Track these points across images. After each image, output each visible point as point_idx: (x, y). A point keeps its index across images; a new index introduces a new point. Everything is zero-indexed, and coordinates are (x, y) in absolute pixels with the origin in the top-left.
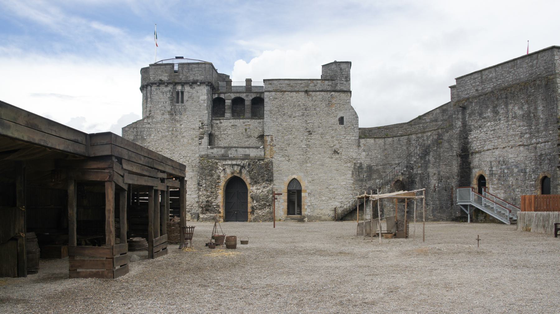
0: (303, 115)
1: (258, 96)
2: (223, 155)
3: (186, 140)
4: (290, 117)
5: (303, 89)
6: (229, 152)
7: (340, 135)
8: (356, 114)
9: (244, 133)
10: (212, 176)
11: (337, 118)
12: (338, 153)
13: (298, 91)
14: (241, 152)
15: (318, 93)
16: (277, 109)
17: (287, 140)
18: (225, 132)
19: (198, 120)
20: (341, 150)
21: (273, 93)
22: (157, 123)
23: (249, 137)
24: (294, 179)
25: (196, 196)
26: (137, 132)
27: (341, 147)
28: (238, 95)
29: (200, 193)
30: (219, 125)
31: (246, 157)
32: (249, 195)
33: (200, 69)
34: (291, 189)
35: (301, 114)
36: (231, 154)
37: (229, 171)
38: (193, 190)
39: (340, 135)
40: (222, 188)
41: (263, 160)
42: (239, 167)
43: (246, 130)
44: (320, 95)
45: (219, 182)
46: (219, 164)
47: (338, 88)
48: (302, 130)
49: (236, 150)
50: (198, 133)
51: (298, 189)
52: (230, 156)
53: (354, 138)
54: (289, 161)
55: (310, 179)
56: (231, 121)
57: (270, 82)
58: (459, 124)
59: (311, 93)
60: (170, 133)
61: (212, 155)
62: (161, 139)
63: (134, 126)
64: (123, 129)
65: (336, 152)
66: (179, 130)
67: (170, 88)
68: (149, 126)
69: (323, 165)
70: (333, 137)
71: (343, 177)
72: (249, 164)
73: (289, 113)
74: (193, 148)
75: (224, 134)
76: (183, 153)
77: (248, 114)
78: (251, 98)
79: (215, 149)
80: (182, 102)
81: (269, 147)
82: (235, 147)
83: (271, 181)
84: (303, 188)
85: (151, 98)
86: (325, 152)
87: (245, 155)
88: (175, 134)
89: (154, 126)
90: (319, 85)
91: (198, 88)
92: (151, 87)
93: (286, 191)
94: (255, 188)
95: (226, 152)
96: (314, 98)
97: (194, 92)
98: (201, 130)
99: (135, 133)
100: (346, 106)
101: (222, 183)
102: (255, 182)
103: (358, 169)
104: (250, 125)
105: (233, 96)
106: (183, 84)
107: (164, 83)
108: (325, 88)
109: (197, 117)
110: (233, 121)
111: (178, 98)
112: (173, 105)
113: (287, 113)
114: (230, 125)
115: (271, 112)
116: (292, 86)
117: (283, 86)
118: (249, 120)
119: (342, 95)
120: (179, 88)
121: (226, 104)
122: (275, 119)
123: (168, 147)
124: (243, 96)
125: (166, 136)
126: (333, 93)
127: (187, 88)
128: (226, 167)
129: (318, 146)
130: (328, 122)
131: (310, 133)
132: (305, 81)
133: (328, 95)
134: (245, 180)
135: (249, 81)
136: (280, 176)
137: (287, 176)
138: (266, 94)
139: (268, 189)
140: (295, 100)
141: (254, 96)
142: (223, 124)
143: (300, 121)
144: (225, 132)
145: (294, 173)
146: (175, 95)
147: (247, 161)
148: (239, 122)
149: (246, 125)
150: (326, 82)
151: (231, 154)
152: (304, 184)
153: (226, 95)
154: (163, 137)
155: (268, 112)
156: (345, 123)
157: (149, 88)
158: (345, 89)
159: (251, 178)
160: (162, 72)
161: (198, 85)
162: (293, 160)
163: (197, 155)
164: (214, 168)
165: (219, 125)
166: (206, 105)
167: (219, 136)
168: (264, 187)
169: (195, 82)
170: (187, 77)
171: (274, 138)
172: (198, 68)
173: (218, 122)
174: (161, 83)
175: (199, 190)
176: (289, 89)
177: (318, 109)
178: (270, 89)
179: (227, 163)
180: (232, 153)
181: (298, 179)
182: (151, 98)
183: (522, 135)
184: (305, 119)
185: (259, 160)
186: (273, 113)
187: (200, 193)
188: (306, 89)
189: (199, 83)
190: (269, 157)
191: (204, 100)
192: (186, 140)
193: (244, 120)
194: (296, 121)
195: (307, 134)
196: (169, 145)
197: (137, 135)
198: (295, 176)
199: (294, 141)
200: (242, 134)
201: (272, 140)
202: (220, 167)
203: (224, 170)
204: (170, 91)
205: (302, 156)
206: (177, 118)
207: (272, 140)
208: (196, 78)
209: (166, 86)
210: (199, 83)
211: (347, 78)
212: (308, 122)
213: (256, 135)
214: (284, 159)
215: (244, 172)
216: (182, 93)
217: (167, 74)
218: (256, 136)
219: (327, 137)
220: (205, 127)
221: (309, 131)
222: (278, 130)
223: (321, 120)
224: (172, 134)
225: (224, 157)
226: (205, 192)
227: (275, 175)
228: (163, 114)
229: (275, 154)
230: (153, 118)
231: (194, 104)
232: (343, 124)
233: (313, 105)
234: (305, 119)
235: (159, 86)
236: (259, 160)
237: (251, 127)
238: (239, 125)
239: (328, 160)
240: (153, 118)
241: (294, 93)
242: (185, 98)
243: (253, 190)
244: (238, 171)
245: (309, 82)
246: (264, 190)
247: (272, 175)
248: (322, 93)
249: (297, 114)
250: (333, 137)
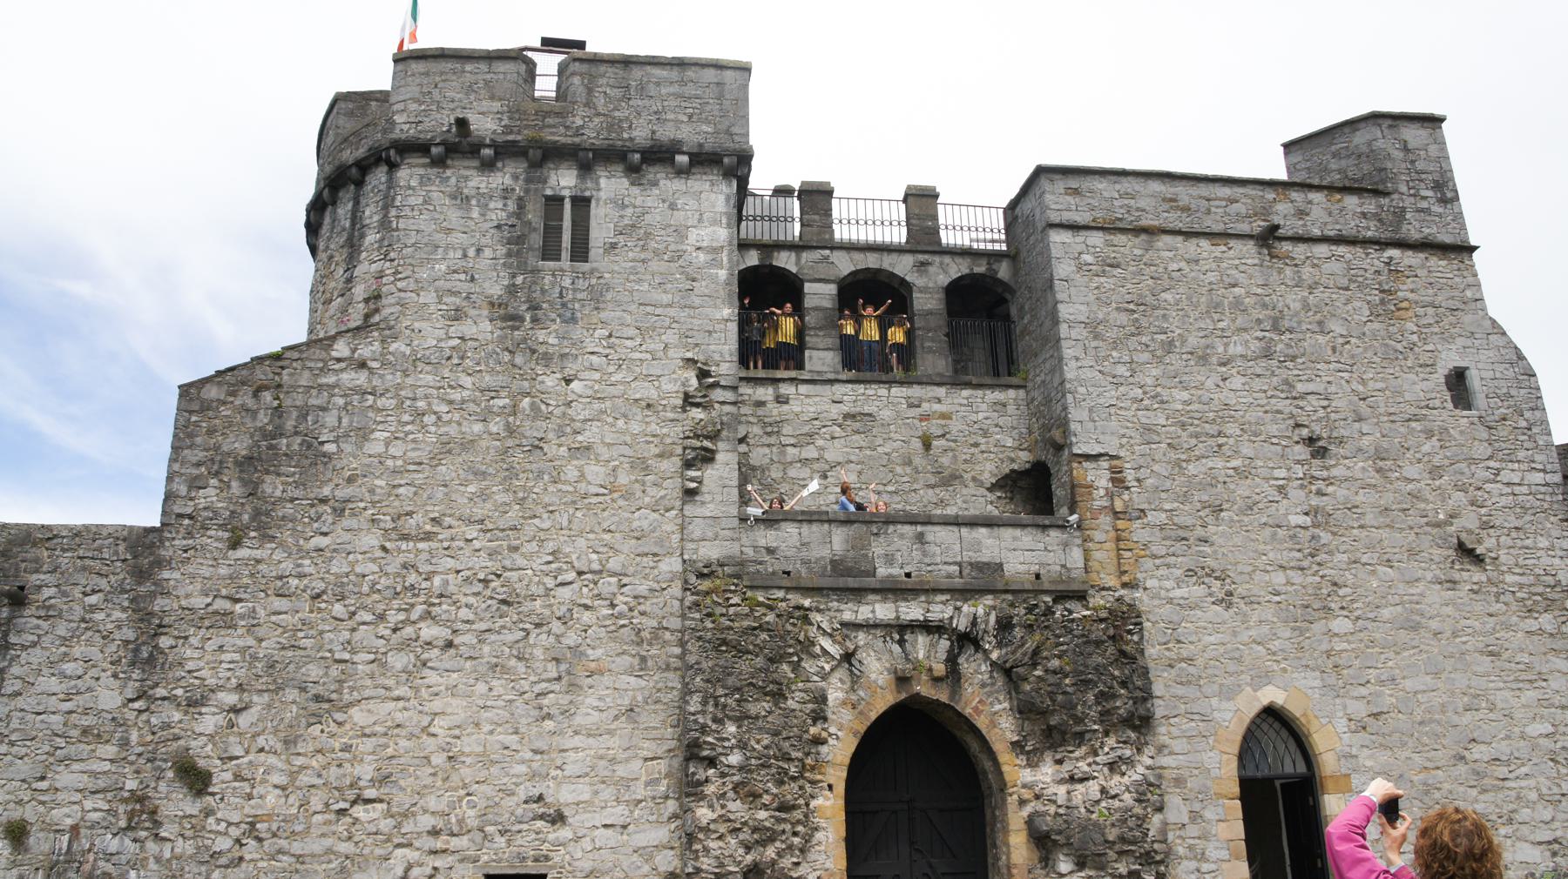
0: (1267, 354)
1: (981, 269)
2: (838, 567)
3: (596, 472)
4: (1204, 359)
5: (1244, 228)
6: (878, 549)
7: (1473, 461)
8: (1521, 357)
9: (917, 461)
10: (778, 696)
11: (1439, 377)
12: (1478, 560)
13: (1226, 235)
14: (948, 550)
15: (1322, 250)
16: (1123, 318)
17: (1202, 487)
18: (809, 452)
19: (677, 354)
20: (1490, 543)
21: (1096, 239)
22: (417, 360)
23: (949, 480)
24: (1272, 714)
25: (662, 834)
26: (278, 411)
27: (1486, 526)
28: (872, 261)
29: (704, 814)
30: (774, 410)
31: (982, 580)
32: (1016, 819)
33: (690, 90)
34: (1264, 772)
35: (1255, 346)
36: (889, 559)
37: (877, 665)
38: (640, 791)
39: (1473, 461)
40: (837, 776)
41: (1081, 596)
42: (944, 644)
43: (927, 446)
44: (1332, 262)
45: (818, 741)
46: (816, 617)
47: (1413, 230)
48: (1273, 429)
49: (920, 538)
50: (674, 433)
51: (1291, 766)
52: (882, 571)
53: (1538, 477)
54: (1227, 601)
55: (1360, 710)
56: (839, 389)
57: (1073, 183)
59: (1286, 247)
60: (496, 426)
61: (772, 565)
62: (435, 460)
63: (261, 374)
64: (186, 390)
65: (1467, 553)
66: (554, 406)
67: (505, 177)
68: (361, 378)
69: (1415, 628)
70: (1436, 472)
71: (1530, 695)
72: (1005, 625)
73: (1193, 341)
74: (644, 519)
75: (805, 462)
76: (579, 551)
77: (933, 361)
78: (944, 280)
79: (791, 529)
80: (581, 251)
81: (1105, 520)
82: (912, 520)
83: (1140, 723)
84: (1328, 763)
85: (385, 224)
86: (1412, 553)
87: (979, 567)
88: (531, 430)
89: (392, 379)
90: (1317, 213)
91: (677, 184)
92: (393, 166)
93: (1236, 790)
94: (1046, 773)
95: (858, 545)
96: (1307, 271)
97: (649, 202)
98: (697, 414)
99: (263, 419)
100: (1467, 318)
101: (839, 750)
102: (1050, 731)
104: (944, 416)
105: (845, 265)
106: (588, 159)
107: (474, 150)
108: (1350, 227)
109: (671, 337)
110: (853, 396)
112: (522, 268)
113: (1184, 342)
114: (835, 411)
115: (1094, 328)
116: (1186, 209)
117: (1142, 204)
118: (941, 391)
119: (1437, 263)
120: (564, 180)
121: (808, 303)
122: (1122, 370)
123: (479, 512)
124: (902, 266)
125: (468, 444)
126: (1394, 253)
127: (610, 185)
128: (862, 637)
129: (1369, 519)
130: (1398, 392)
131: (1317, 448)
132: (1249, 190)
133: (1374, 260)
134: (981, 723)
135: (921, 201)
136: (1190, 692)
137: (1229, 694)
138: (1057, 237)
139: (1135, 775)
140: (1212, 277)
141: (957, 269)
142: (795, 406)
143: (1257, 384)
144: (809, 452)
145: (1262, 678)
146: (534, 215)
147: (989, 600)
149: (924, 418)
150: (1351, 201)
151: (889, 559)
152: (1331, 742)
153: (806, 256)
154: (446, 447)
155: (1079, 332)
156: (1480, 400)
157: (378, 177)
158: (1447, 239)
159: (1026, 710)
160: (470, 89)
161: (682, 172)
162: (1250, 601)
163: (672, 565)
164: (789, 646)
165: (774, 410)
166: (723, 274)
167: (775, 473)
168: (1112, 766)
170: (614, 125)
171: (1130, 475)
172: (682, 83)
173: (765, 393)
175: (690, 790)
176: (1174, 220)
177: (1337, 327)
178: (1082, 218)
179: (864, 612)
180: (894, 554)
181: (1295, 709)
182: (385, 224)
184: (1284, 373)
185: (1061, 597)
186: (1111, 334)
187: (704, 814)
188: (1258, 226)
189: (682, 159)
190: (1112, 581)
191: (715, 250)
192: (596, 472)
193: (916, 391)
194: (1237, 382)
195: (1302, 452)
196: (484, 495)
197: (279, 433)
198: (1272, 695)
199: (1242, 489)
200: (909, 463)
201: (1118, 481)
202: (826, 643)
203: (848, 657)
204: (506, 193)
205: (1296, 577)
206: (547, 337)
207: (1118, 481)
208: (666, 133)
209: (488, 166)
210: (682, 159)
211: (1445, 190)
212: (1301, 388)
213: (989, 470)
214: (1200, 591)
215: (975, 669)
216: (582, 204)
217: (496, 105)
218: (989, 479)
219: (1411, 471)
220: (718, 395)
221: (1311, 441)
222: (1148, 429)
223: (1363, 382)
224: (511, 431)
225: (849, 581)
226: (736, 807)
227: (1158, 689)
228: (457, 315)
229: (1148, 563)
230: (389, 332)
231: (654, 265)
232: (1468, 406)
233: (1306, 307)
234: (1284, 373)
235: (439, 162)
236: (1061, 597)
237: (955, 426)
238: (886, 414)
239: (1436, 595)
240: (389, 332)
241: (1204, 243)
242: (600, 230)
243: (1034, 784)
244: (940, 669)
245: (1270, 195)
246: (1115, 783)
247: (1146, 695)
248: (1341, 250)
249: (1236, 349)
250: (1436, 472)
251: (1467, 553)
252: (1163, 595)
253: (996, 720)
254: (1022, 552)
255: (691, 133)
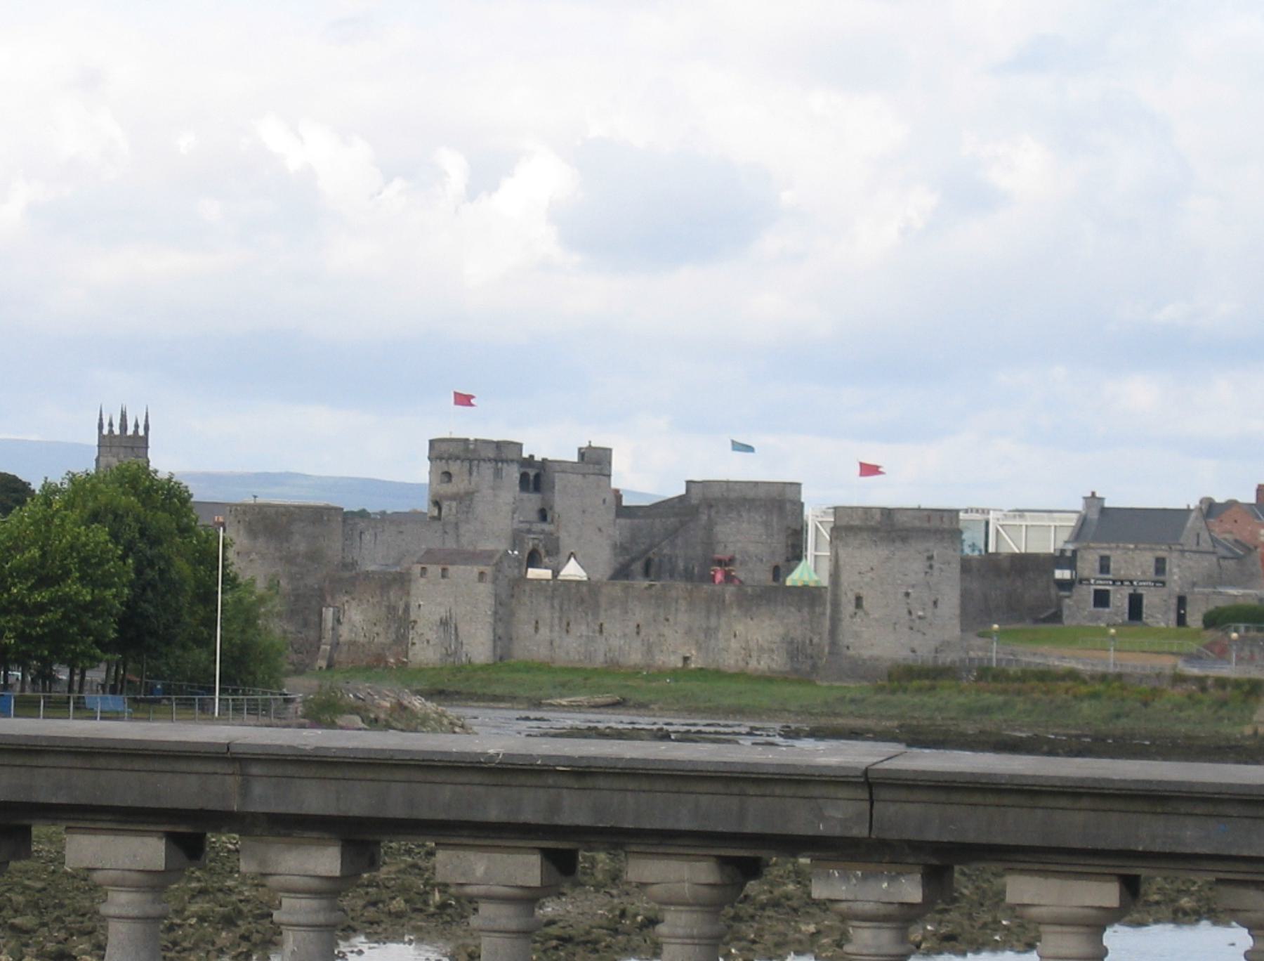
31: (542, 532)
58: (705, 517)
103: (615, 546)
105: (523, 470)
106: (502, 461)
111: (498, 474)
148: (525, 495)
169: (512, 461)
174: (490, 460)
183: (761, 536)
211: (610, 463)
225: (529, 531)
251: (600, 530)
252: (563, 535)
253: (542, 551)
254: (546, 527)
255: (515, 457)
